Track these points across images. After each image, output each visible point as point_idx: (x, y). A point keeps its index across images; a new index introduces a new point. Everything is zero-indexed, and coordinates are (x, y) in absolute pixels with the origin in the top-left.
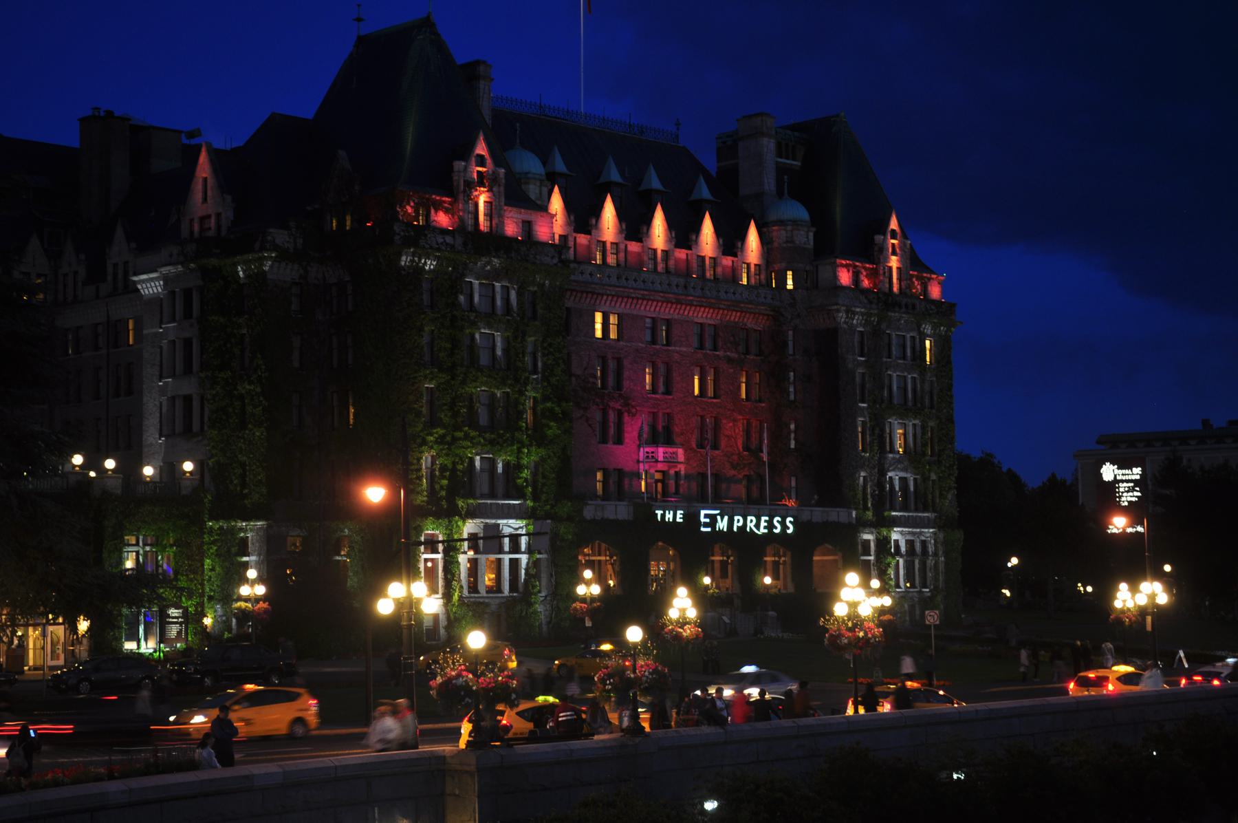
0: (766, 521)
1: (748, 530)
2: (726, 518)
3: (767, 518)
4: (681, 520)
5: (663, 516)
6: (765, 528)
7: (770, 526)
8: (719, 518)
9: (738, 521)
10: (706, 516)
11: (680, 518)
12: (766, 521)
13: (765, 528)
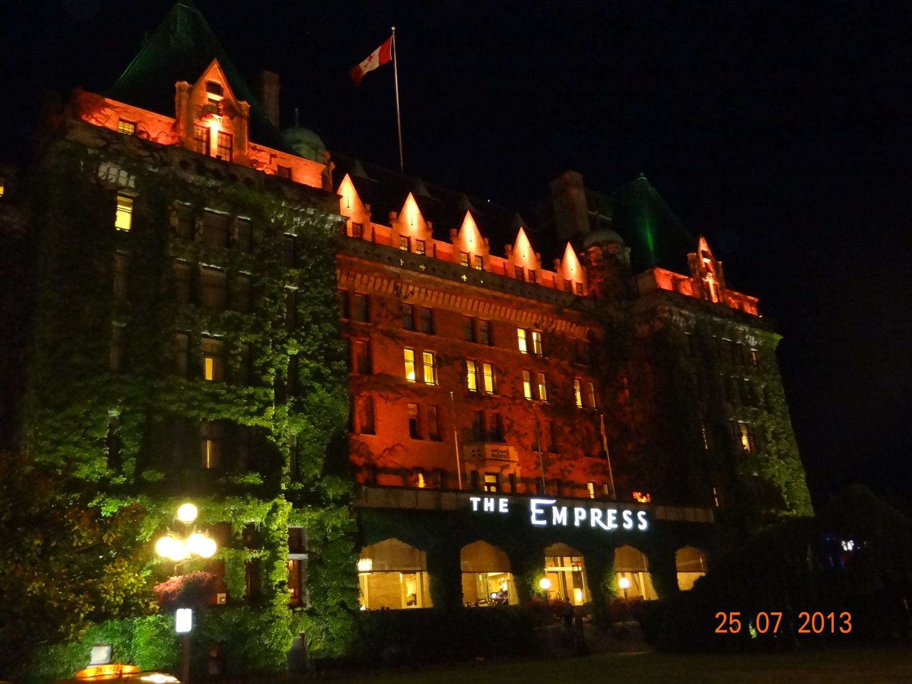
0: (613, 515)
1: (593, 524)
2: (564, 509)
3: (615, 511)
4: (506, 510)
5: (481, 505)
6: (614, 522)
7: (620, 520)
8: (555, 509)
9: (580, 514)
10: (539, 506)
11: (504, 508)
12: (613, 515)
13: (614, 522)
